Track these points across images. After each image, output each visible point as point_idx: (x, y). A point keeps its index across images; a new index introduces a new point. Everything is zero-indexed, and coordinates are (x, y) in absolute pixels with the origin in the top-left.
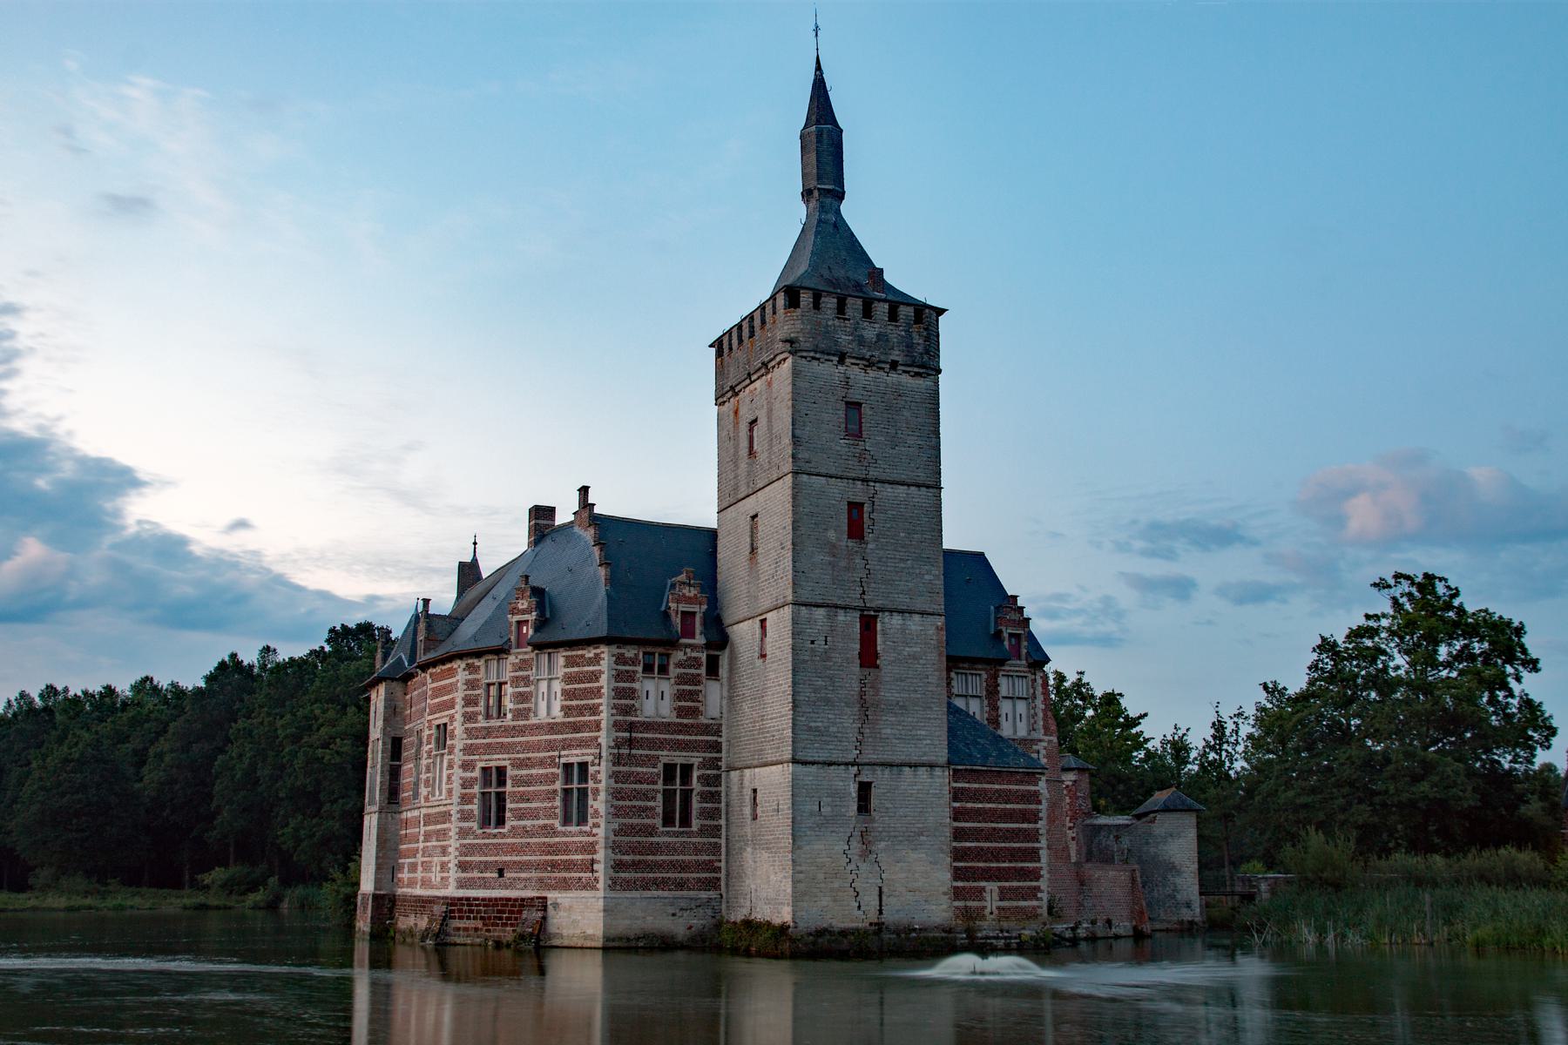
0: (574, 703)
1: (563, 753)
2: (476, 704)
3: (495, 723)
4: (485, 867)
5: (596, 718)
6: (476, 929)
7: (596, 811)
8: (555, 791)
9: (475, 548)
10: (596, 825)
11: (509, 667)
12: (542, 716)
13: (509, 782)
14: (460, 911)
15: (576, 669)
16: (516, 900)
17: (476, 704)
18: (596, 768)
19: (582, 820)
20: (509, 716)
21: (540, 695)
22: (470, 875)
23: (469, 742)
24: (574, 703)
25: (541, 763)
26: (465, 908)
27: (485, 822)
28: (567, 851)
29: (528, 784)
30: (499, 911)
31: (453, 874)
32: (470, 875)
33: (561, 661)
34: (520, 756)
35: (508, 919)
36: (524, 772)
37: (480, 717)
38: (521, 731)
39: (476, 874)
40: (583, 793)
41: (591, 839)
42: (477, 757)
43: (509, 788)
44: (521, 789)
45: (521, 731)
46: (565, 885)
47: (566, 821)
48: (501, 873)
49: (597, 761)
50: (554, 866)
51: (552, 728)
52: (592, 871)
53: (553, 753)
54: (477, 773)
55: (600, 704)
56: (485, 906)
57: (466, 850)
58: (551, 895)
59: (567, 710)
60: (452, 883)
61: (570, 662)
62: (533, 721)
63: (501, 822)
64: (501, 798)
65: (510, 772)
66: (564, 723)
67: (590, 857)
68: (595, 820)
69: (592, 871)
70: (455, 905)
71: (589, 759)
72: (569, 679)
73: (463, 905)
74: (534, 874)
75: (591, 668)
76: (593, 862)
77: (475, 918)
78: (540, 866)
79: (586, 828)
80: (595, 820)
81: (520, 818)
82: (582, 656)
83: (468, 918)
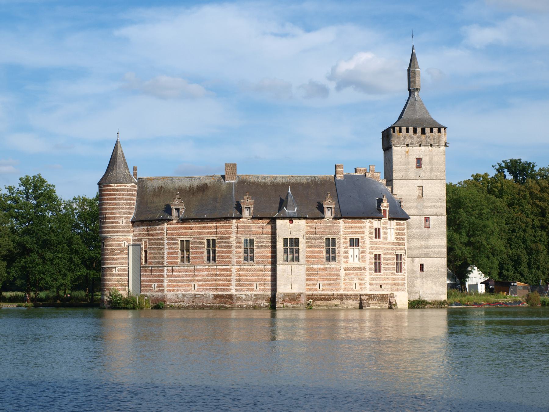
0: (398, 237)
1: (396, 251)
2: (372, 234)
3: (378, 240)
4: (377, 284)
5: (404, 242)
6: (376, 303)
7: (405, 269)
8: (394, 262)
9: (118, 136)
10: (405, 273)
11: (381, 224)
12: (389, 240)
13: (382, 259)
14: (371, 298)
15: (398, 226)
16: (386, 294)
17: (372, 234)
18: (405, 256)
19: (401, 271)
20: (381, 238)
21: (393, 234)
22: (372, 287)
23: (371, 246)
24: (398, 237)
25: (391, 254)
26: (373, 297)
27: (376, 271)
28: (398, 280)
29: (388, 260)
30: (382, 298)
31: (368, 287)
32: (372, 287)
33: (395, 224)
34: (386, 251)
35: (384, 300)
36: (386, 256)
37: (374, 238)
38: (385, 244)
39: (374, 287)
40: (401, 263)
41: (404, 277)
42: (373, 251)
43: (382, 261)
44: (386, 261)
45: (385, 244)
46: (398, 290)
47: (397, 271)
48: (381, 286)
49: (405, 254)
50: (395, 284)
51: (393, 244)
52: (404, 286)
53: (393, 251)
54: (373, 256)
55: (405, 238)
56: (378, 296)
57: (372, 279)
58: (395, 293)
59: (397, 238)
60: (368, 290)
61: (397, 224)
62: (388, 241)
63: (380, 271)
64: (380, 263)
65: (382, 256)
66: (396, 242)
67: (403, 282)
68: (405, 271)
69: (404, 286)
70: (370, 296)
71: (402, 254)
72: (397, 229)
73: (372, 296)
74: (390, 287)
75: (402, 227)
76: (404, 283)
77: (375, 300)
78: (391, 285)
79: (402, 274)
80: (405, 271)
81: (386, 270)
82: (400, 223)
83: (374, 300)
